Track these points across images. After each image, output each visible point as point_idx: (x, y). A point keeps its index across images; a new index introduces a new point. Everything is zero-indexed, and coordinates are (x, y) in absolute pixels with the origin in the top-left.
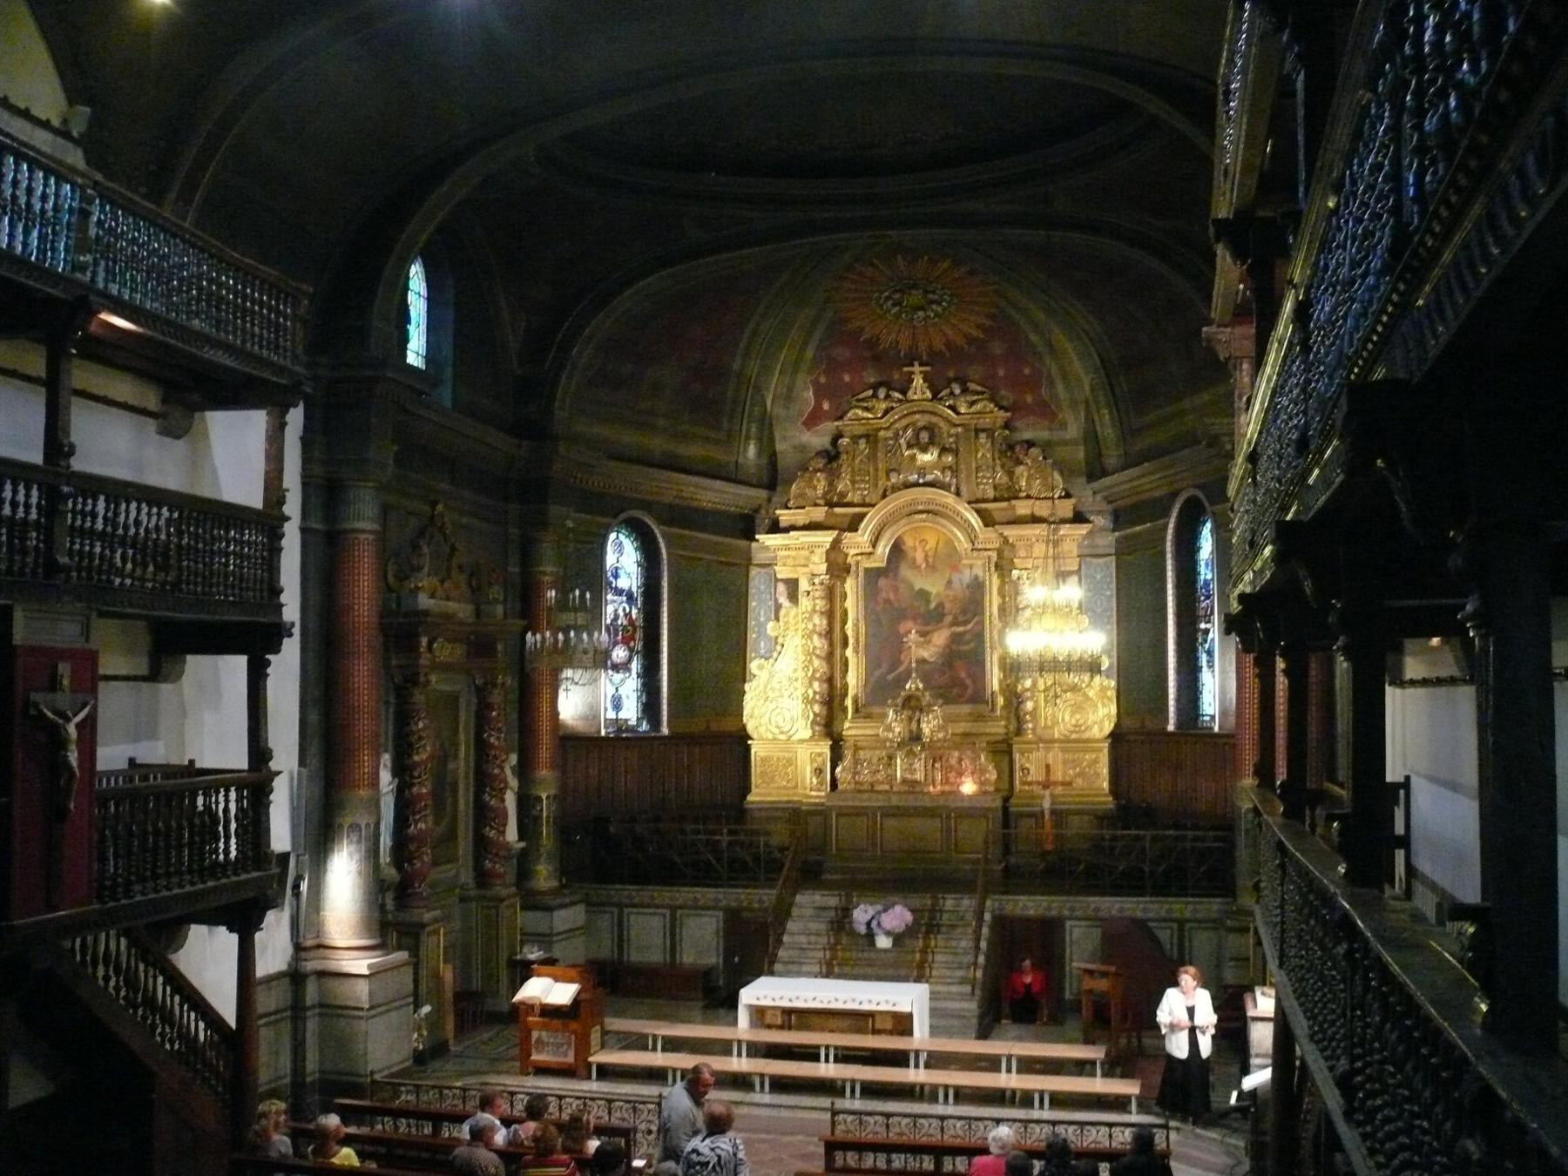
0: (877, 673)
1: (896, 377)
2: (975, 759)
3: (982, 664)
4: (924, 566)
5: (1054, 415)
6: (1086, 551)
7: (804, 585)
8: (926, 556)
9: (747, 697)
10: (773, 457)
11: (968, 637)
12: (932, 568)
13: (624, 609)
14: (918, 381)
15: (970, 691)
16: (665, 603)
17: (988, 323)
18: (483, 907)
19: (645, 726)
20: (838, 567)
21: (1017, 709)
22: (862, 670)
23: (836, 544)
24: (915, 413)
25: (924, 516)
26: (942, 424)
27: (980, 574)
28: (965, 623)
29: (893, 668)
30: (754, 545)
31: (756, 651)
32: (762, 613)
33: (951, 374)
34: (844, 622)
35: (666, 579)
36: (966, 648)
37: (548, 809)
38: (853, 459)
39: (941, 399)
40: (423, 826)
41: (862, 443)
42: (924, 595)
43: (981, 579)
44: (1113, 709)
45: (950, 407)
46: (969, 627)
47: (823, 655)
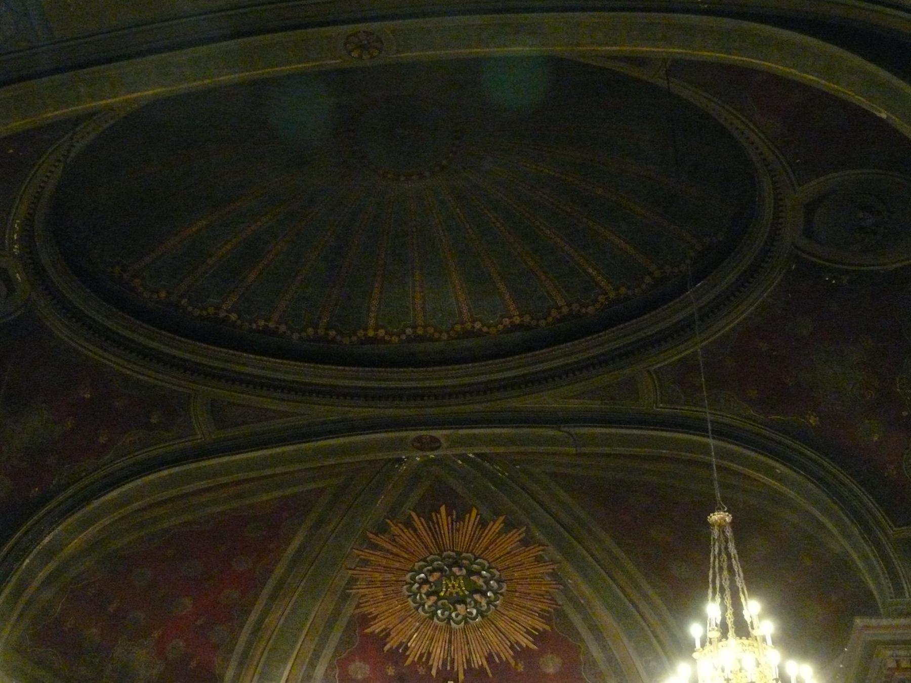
17: (541, 625)
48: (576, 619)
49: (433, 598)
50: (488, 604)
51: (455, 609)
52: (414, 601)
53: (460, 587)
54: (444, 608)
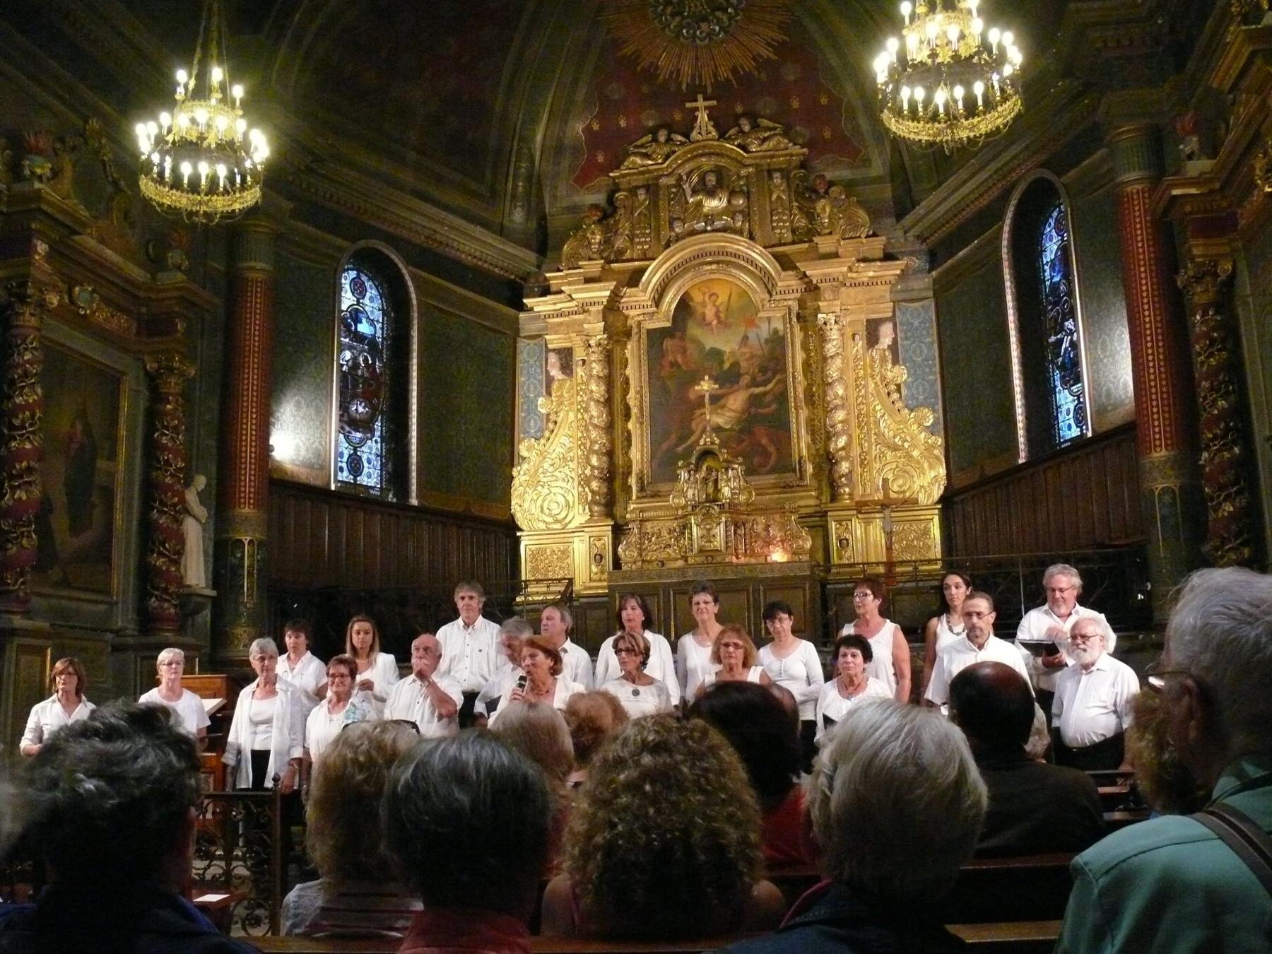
0: (665, 446)
1: (678, 117)
2: (783, 527)
3: (787, 429)
4: (715, 322)
5: (859, 152)
6: (900, 297)
7: (579, 354)
8: (717, 315)
9: (516, 482)
10: (543, 218)
11: (769, 398)
12: (724, 324)
13: (366, 360)
14: (703, 117)
15: (773, 458)
16: (415, 354)
18: (143, 658)
19: (391, 497)
20: (618, 331)
21: (830, 471)
22: (647, 443)
23: (615, 297)
24: (702, 155)
25: (714, 267)
26: (733, 168)
27: (780, 326)
28: (765, 383)
29: (683, 439)
30: (522, 315)
31: (525, 432)
32: (532, 388)
33: (739, 109)
34: (626, 391)
35: (415, 327)
36: (766, 410)
37: (251, 556)
38: (632, 213)
39: (729, 138)
40: (24, 497)
41: (642, 194)
42: (717, 354)
43: (781, 333)
44: (942, 471)
45: (739, 146)
46: (770, 386)
47: (602, 424)
48: (811, 26)
49: (678, 19)
50: (730, 19)
51: (699, 28)
52: (660, 21)
53: (702, 5)
54: (688, 26)
